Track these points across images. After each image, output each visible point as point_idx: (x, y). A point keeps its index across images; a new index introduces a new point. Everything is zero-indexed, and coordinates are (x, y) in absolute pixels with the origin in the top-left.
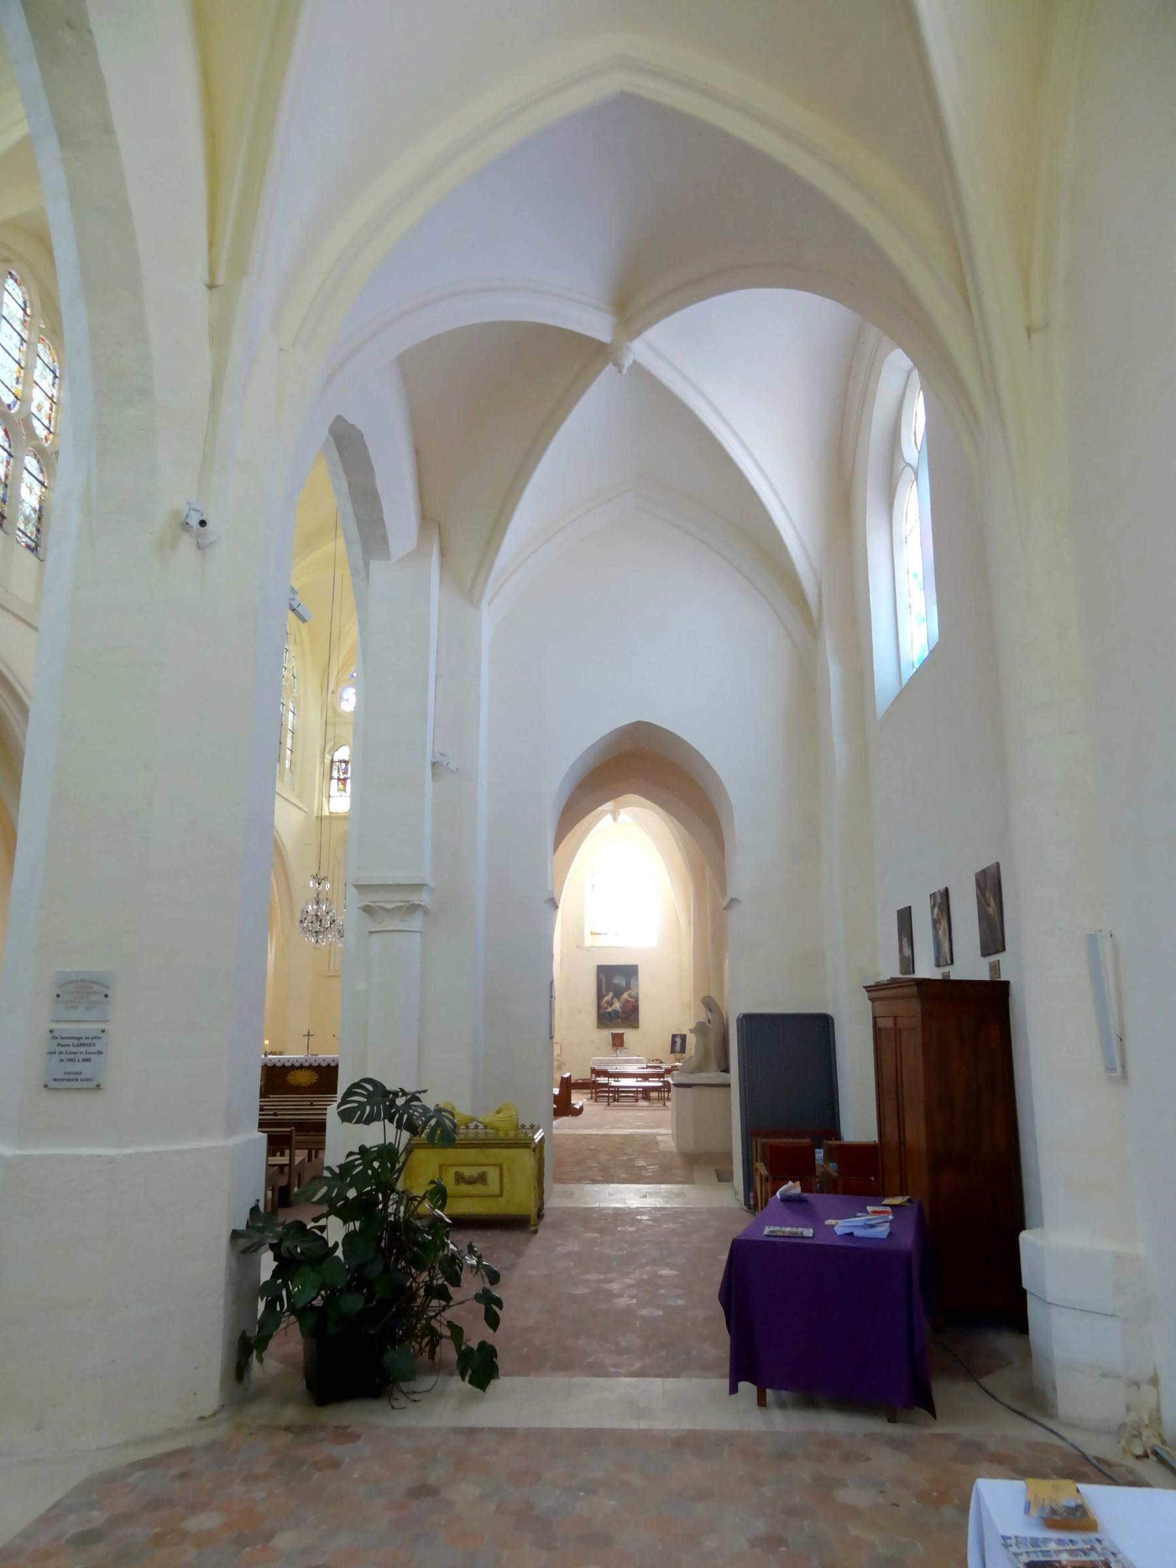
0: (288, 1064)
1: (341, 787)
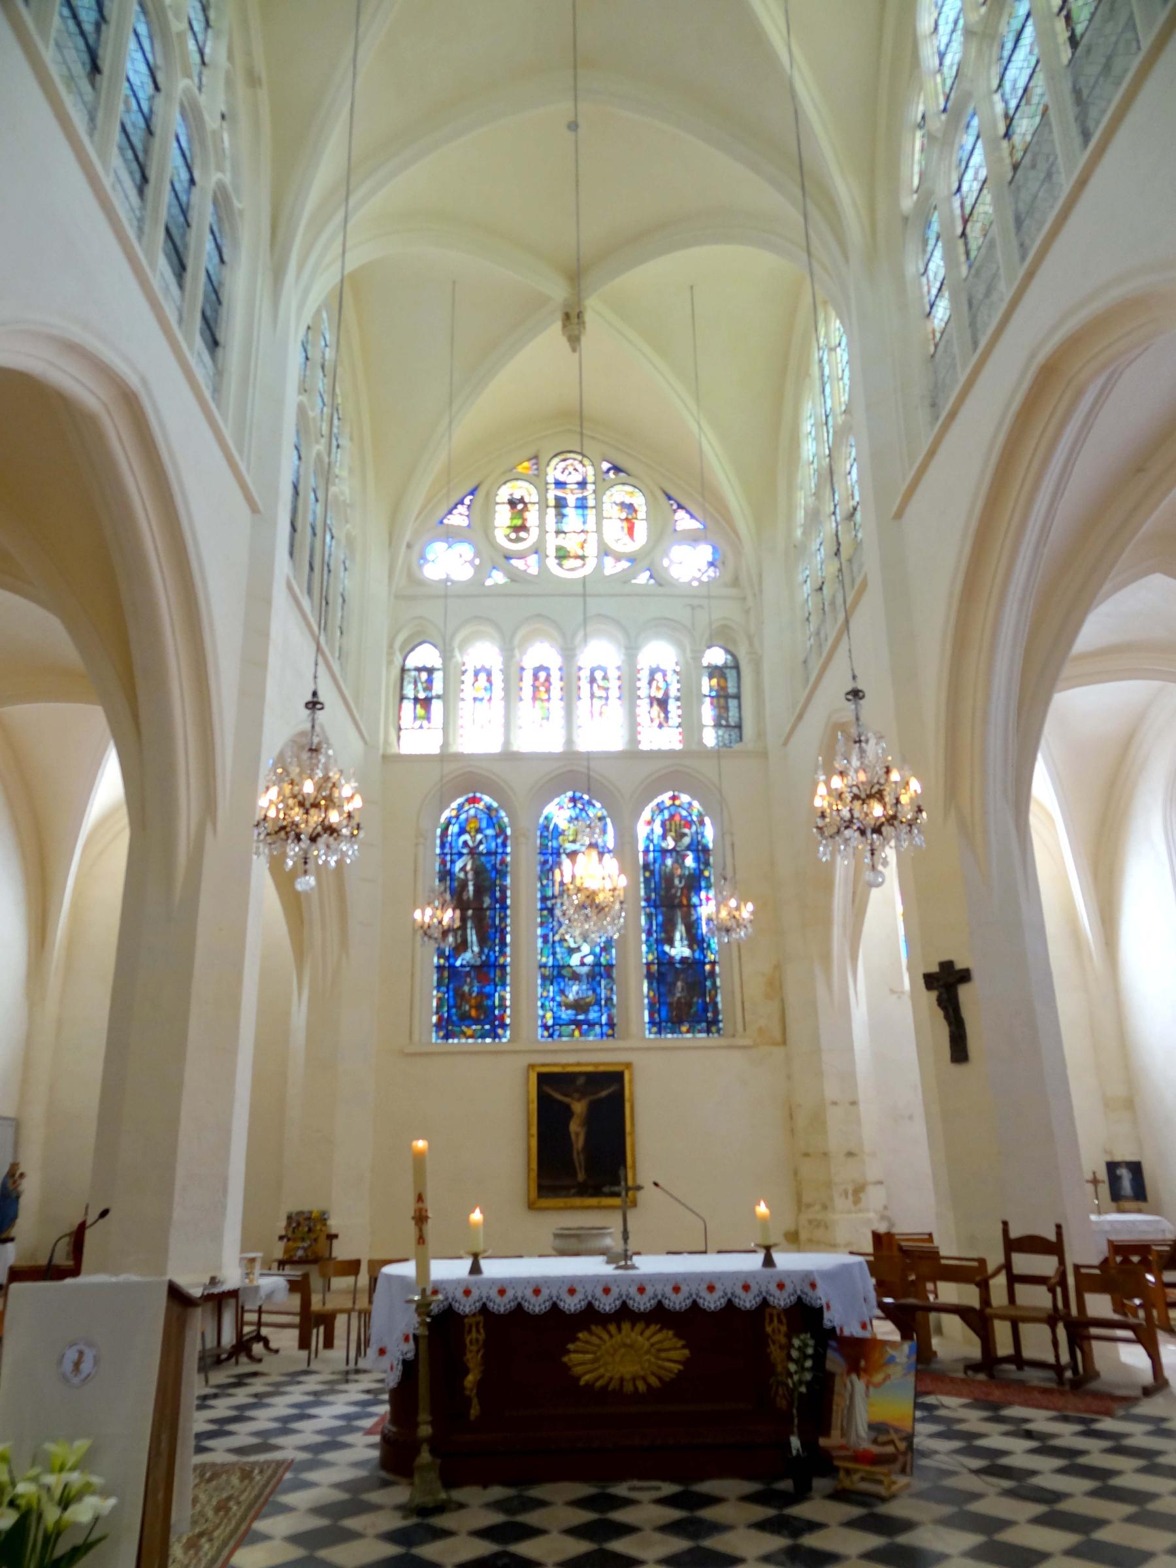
0: (571, 1304)
1: (420, 711)
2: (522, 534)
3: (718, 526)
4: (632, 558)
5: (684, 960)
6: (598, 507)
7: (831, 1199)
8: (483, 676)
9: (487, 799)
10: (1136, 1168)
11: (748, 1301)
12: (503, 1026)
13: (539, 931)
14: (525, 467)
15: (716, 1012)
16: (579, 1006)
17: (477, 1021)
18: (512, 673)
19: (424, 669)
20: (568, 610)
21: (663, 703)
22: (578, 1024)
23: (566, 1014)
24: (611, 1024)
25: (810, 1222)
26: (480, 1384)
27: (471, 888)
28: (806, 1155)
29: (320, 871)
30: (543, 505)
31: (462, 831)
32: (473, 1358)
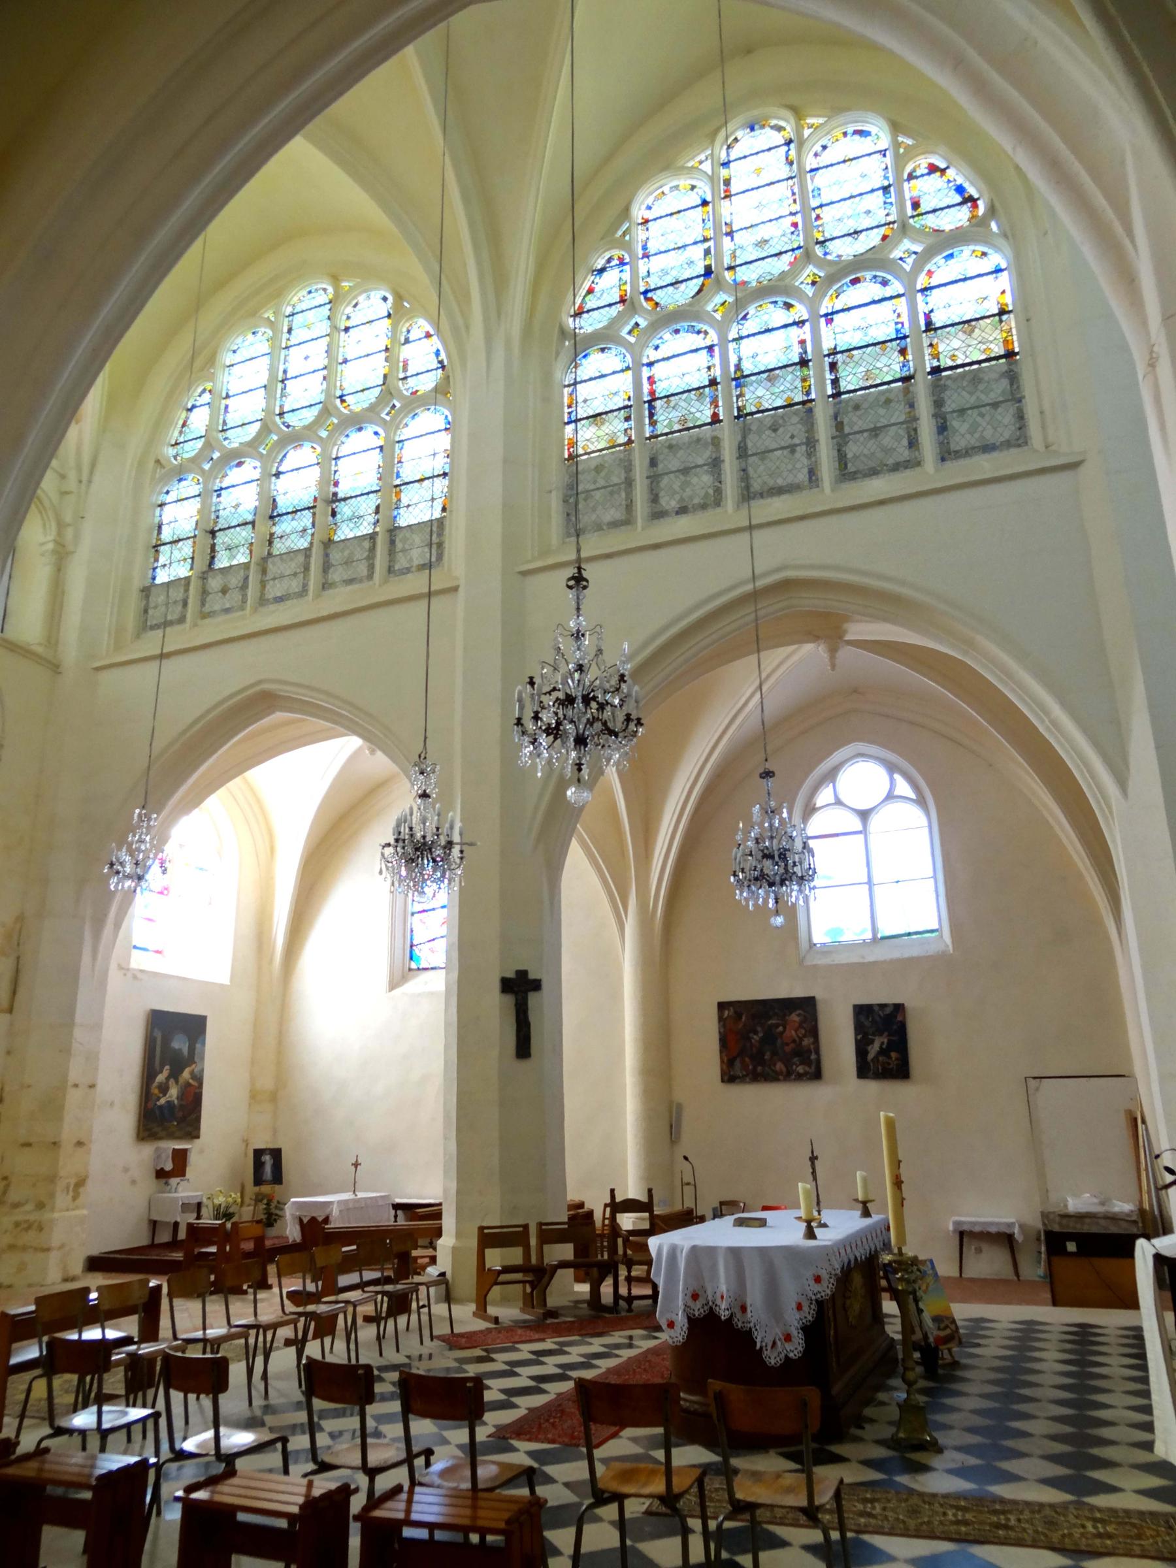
7: (52, 1195)
10: (276, 1154)
25: (17, 1224)
28: (29, 1145)
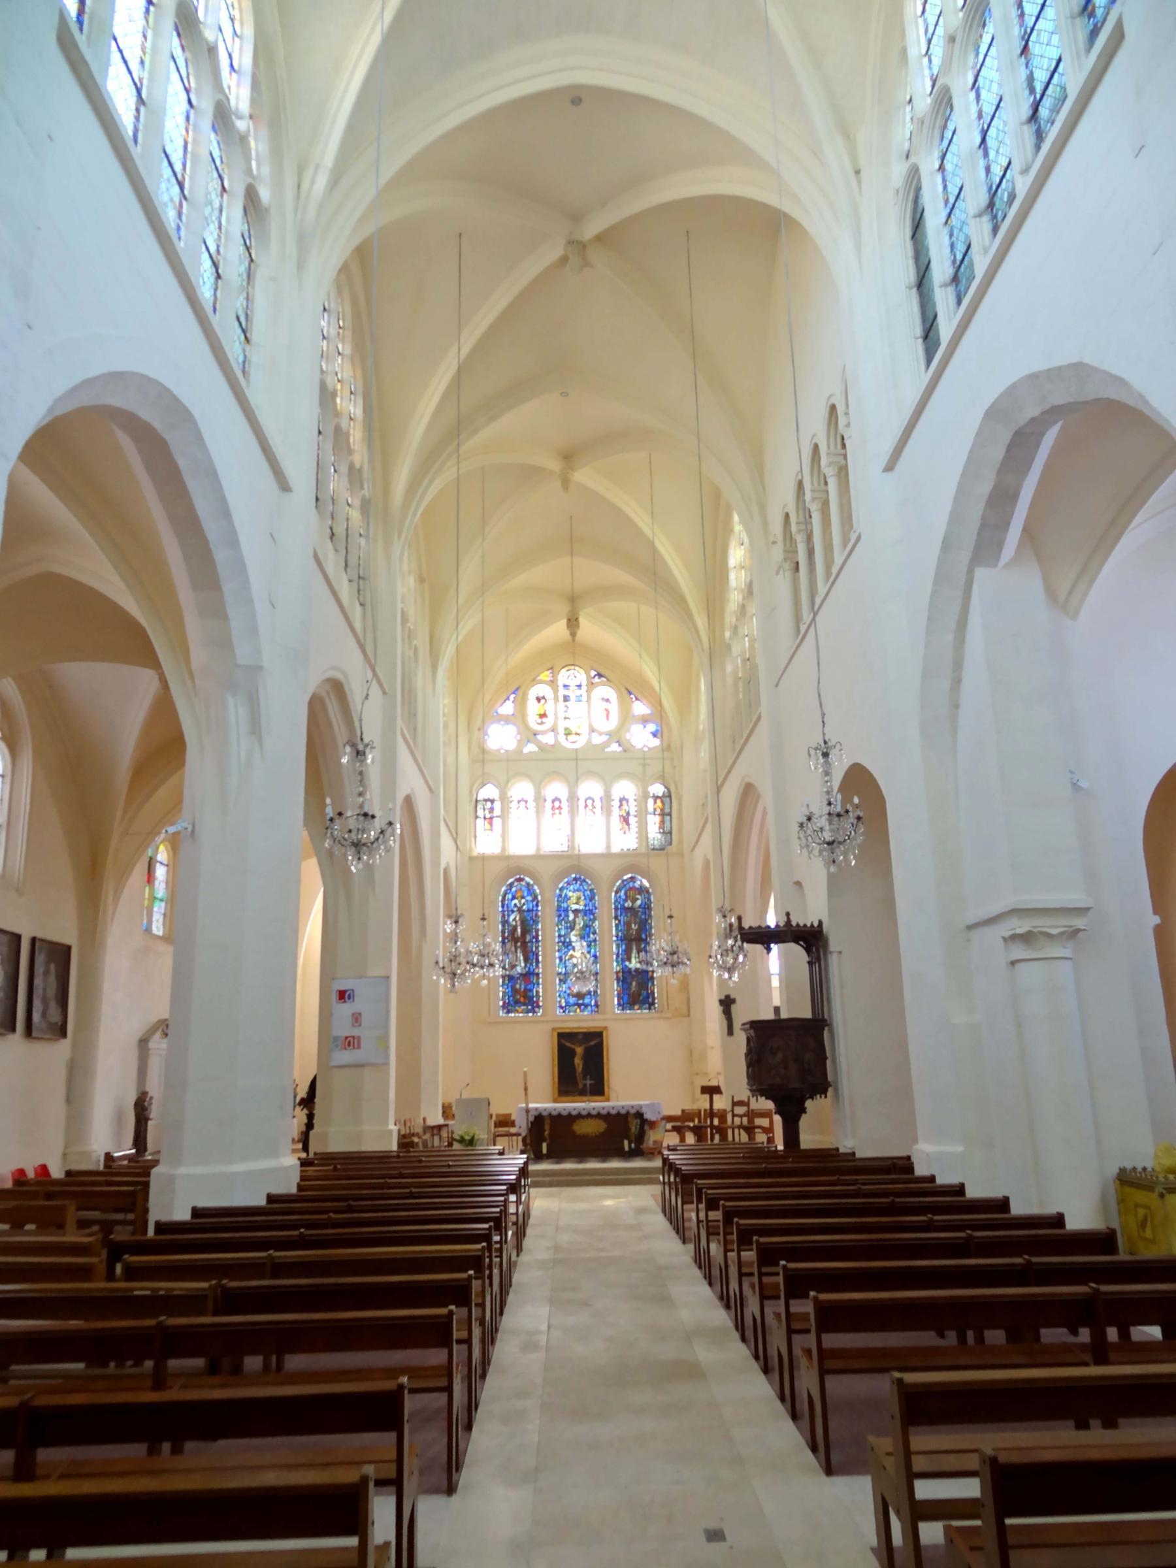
0: (574, 1113)
1: (488, 826)
2: (544, 720)
3: (658, 714)
4: (609, 734)
5: (637, 970)
6: (589, 700)
8: (523, 803)
9: (527, 879)
11: (623, 1112)
12: (538, 1007)
13: (557, 954)
14: (546, 676)
15: (654, 999)
16: (580, 996)
17: (524, 1004)
18: (539, 799)
19: (489, 800)
20: (572, 765)
21: (625, 820)
22: (579, 1005)
23: (572, 1000)
24: (597, 1005)
26: (550, 1135)
27: (519, 930)
29: (489, 979)
30: (556, 699)
31: (514, 898)
32: (547, 1127)
